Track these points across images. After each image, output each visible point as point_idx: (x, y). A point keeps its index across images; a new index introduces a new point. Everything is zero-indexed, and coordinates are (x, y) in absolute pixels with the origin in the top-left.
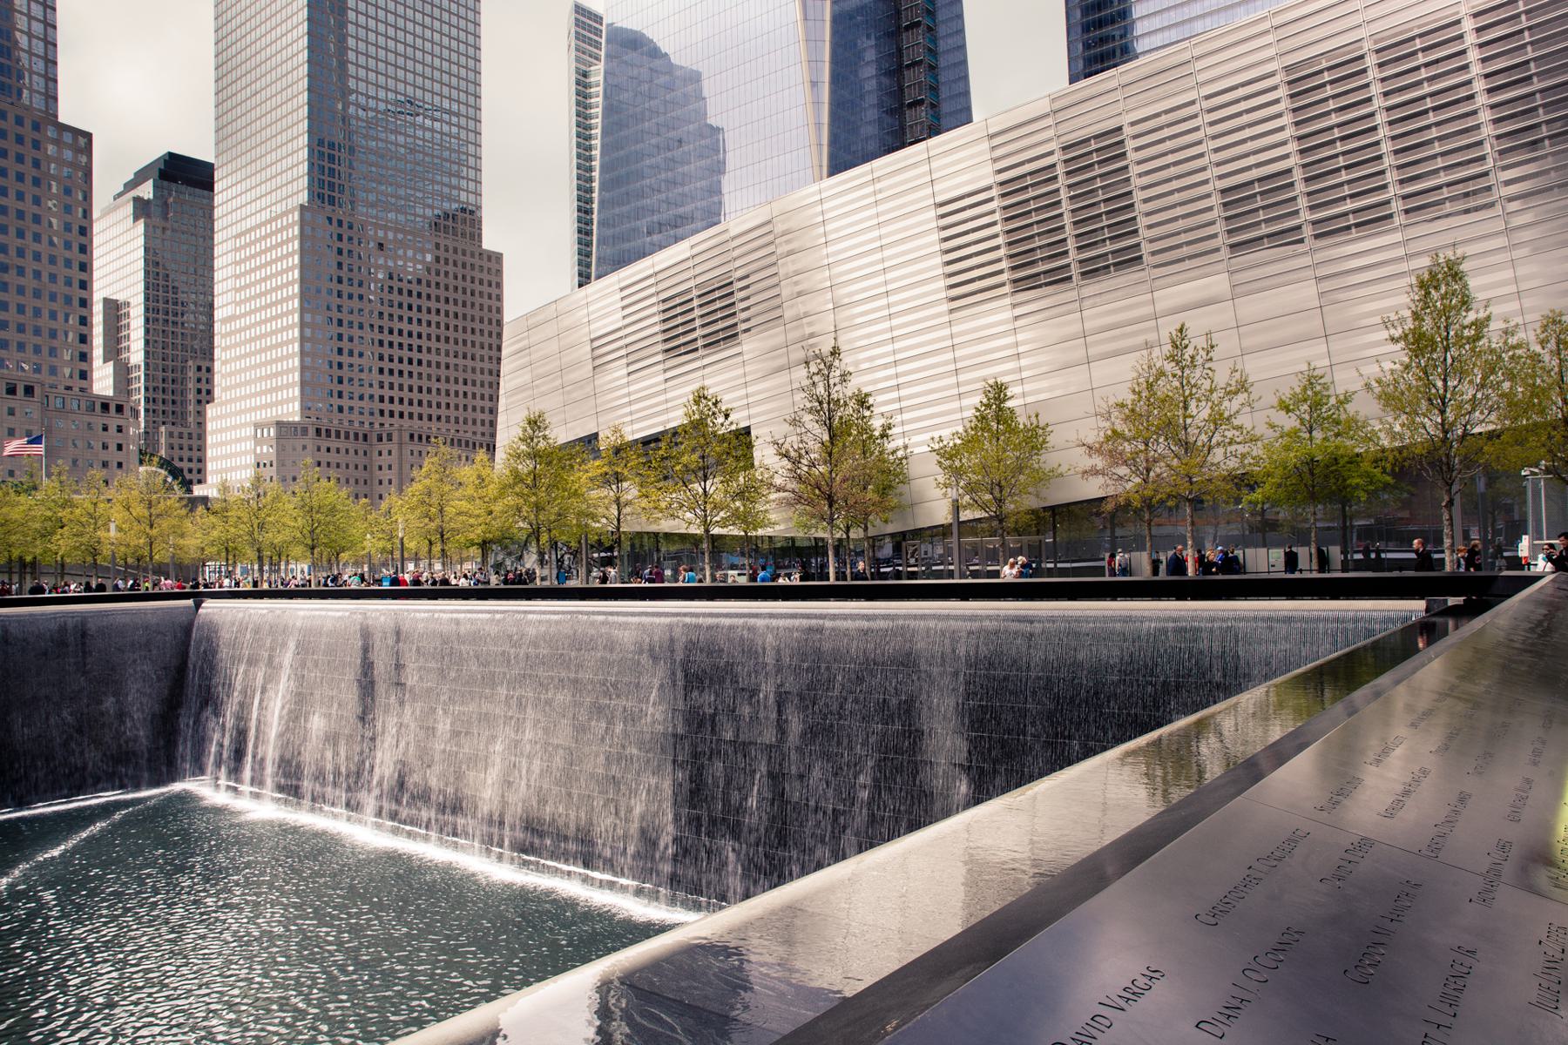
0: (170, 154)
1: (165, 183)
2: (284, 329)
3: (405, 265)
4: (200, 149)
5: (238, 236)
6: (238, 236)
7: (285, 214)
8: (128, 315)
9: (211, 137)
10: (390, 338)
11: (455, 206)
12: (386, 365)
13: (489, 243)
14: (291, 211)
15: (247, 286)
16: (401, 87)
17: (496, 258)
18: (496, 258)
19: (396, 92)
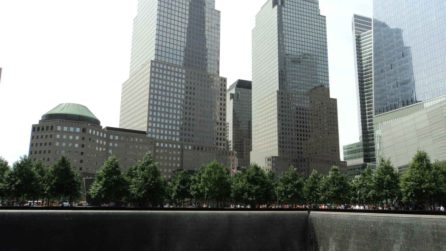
0: (239, 80)
1: (238, 88)
2: (273, 128)
3: (304, 105)
4: (247, 77)
5: (259, 101)
6: (259, 101)
7: (273, 93)
8: (228, 126)
9: (251, 74)
10: (303, 129)
11: (319, 84)
12: (299, 137)
13: (332, 95)
14: (274, 93)
15: (262, 116)
16: (301, 51)
17: (335, 100)
18: (335, 100)
19: (300, 52)
